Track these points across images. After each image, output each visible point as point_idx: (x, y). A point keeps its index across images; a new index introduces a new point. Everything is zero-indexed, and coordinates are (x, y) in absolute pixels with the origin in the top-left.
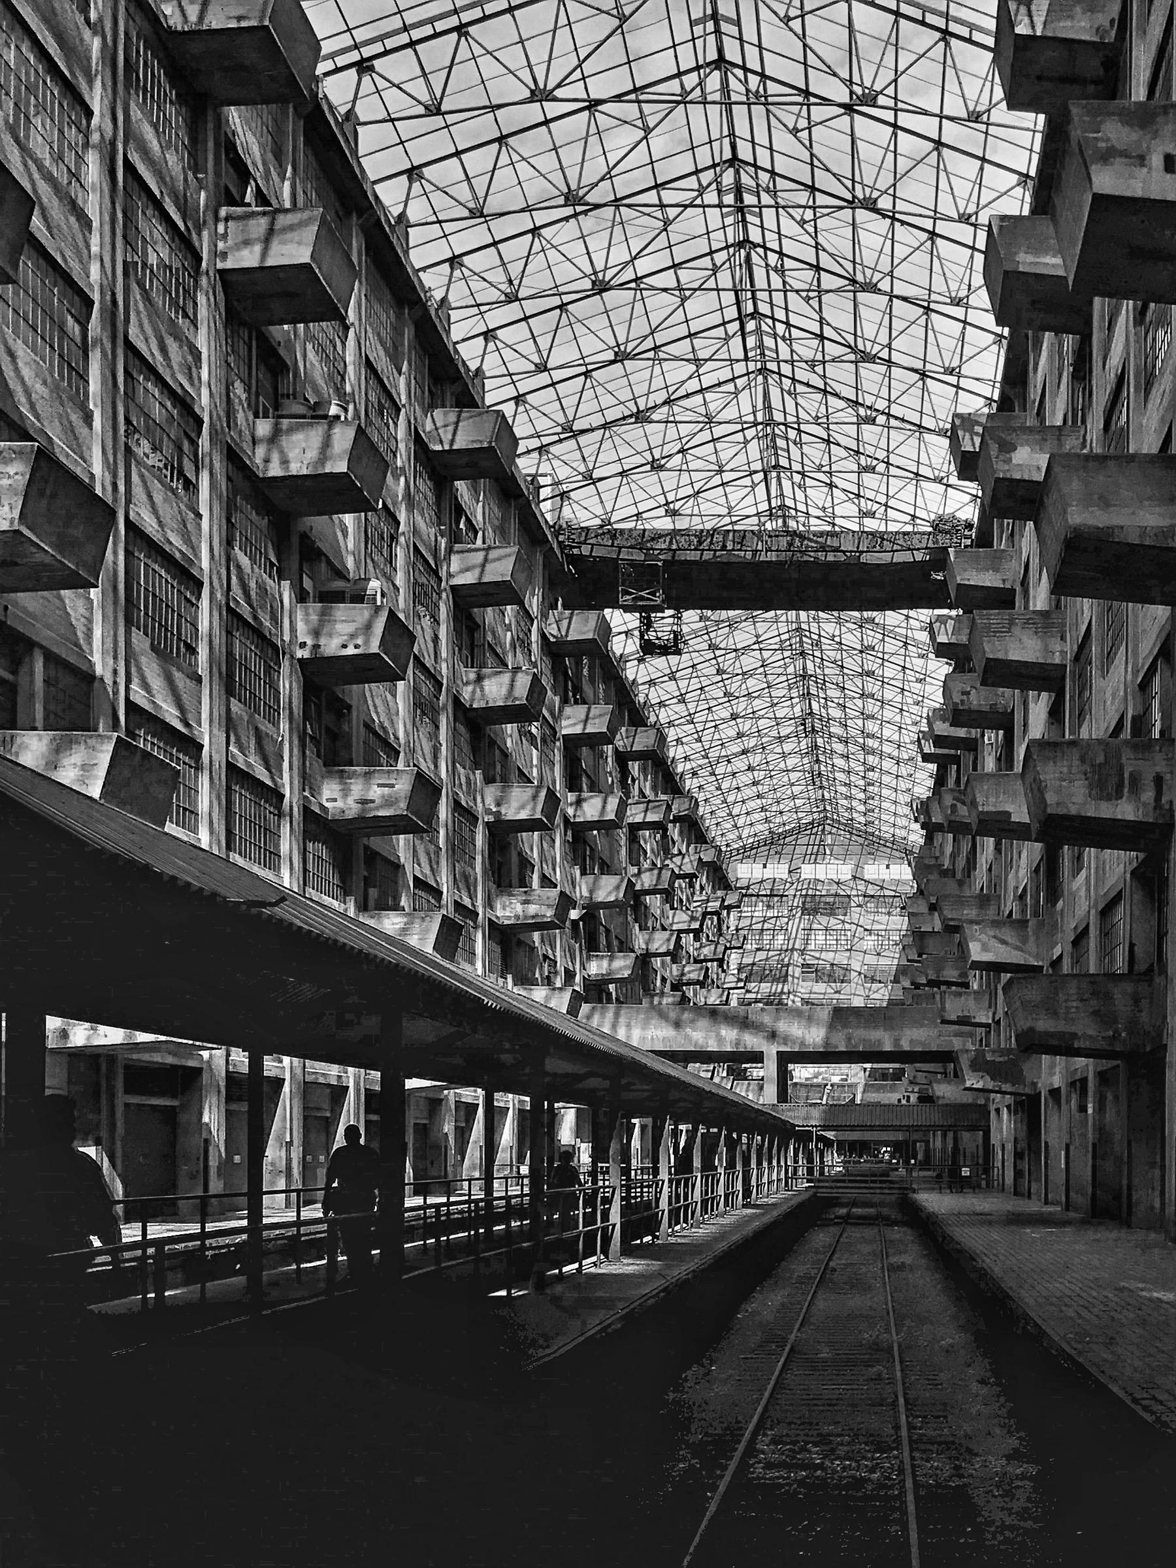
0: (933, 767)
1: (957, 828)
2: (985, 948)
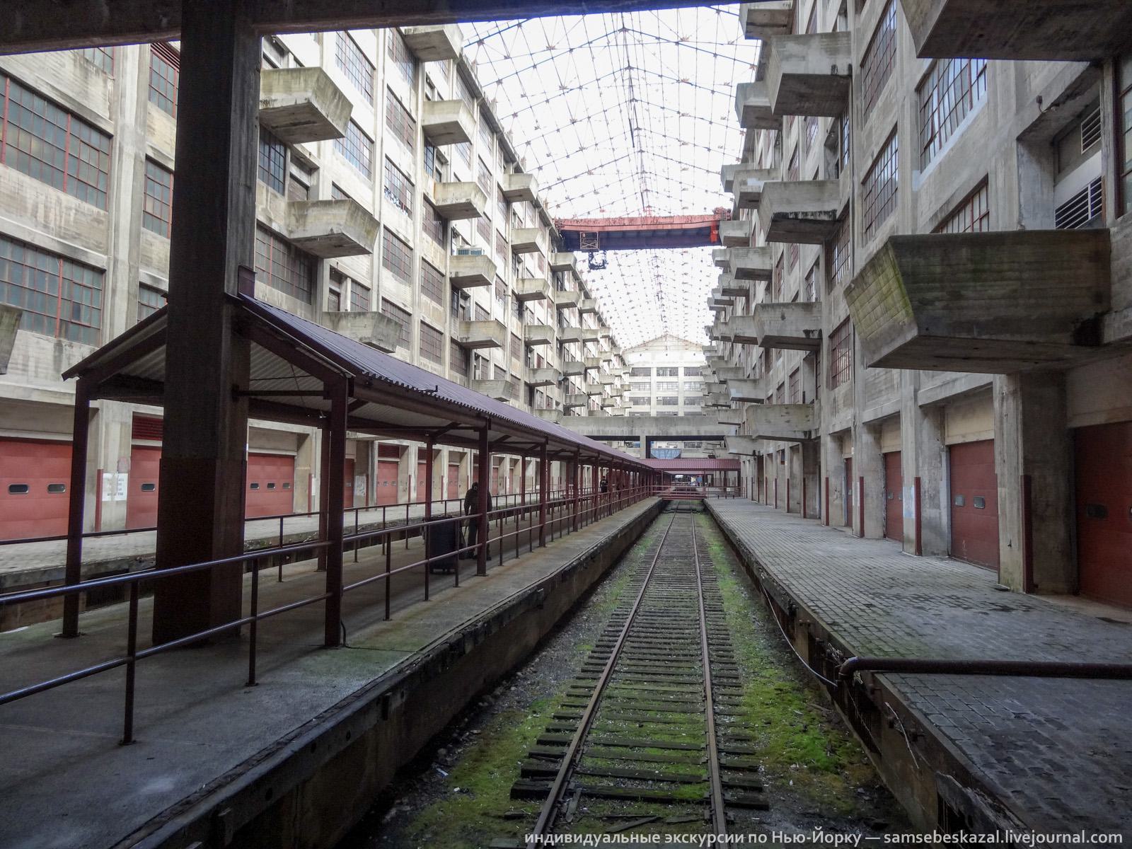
0: (714, 312)
1: (725, 339)
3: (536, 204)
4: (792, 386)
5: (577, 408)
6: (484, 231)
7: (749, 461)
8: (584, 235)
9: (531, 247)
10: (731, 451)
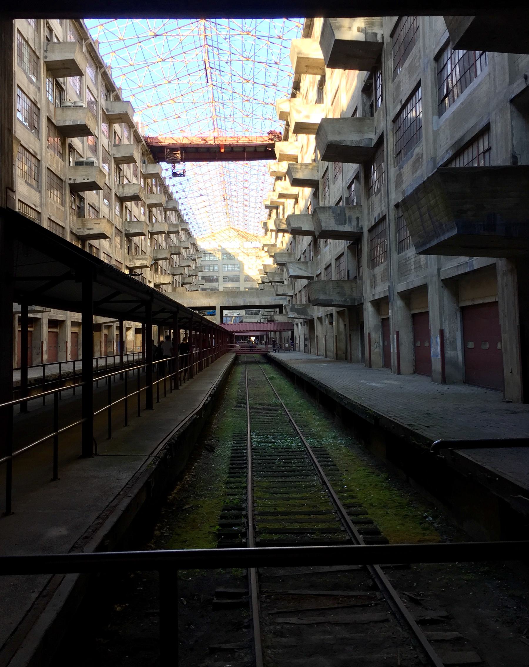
0: (268, 210)
2: (294, 271)
3: (131, 126)
4: (337, 267)
5: (164, 286)
6: (94, 149)
7: (301, 323)
8: (168, 150)
9: (130, 160)
10: (289, 316)
